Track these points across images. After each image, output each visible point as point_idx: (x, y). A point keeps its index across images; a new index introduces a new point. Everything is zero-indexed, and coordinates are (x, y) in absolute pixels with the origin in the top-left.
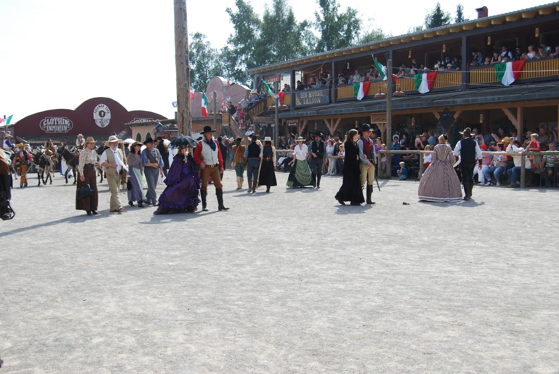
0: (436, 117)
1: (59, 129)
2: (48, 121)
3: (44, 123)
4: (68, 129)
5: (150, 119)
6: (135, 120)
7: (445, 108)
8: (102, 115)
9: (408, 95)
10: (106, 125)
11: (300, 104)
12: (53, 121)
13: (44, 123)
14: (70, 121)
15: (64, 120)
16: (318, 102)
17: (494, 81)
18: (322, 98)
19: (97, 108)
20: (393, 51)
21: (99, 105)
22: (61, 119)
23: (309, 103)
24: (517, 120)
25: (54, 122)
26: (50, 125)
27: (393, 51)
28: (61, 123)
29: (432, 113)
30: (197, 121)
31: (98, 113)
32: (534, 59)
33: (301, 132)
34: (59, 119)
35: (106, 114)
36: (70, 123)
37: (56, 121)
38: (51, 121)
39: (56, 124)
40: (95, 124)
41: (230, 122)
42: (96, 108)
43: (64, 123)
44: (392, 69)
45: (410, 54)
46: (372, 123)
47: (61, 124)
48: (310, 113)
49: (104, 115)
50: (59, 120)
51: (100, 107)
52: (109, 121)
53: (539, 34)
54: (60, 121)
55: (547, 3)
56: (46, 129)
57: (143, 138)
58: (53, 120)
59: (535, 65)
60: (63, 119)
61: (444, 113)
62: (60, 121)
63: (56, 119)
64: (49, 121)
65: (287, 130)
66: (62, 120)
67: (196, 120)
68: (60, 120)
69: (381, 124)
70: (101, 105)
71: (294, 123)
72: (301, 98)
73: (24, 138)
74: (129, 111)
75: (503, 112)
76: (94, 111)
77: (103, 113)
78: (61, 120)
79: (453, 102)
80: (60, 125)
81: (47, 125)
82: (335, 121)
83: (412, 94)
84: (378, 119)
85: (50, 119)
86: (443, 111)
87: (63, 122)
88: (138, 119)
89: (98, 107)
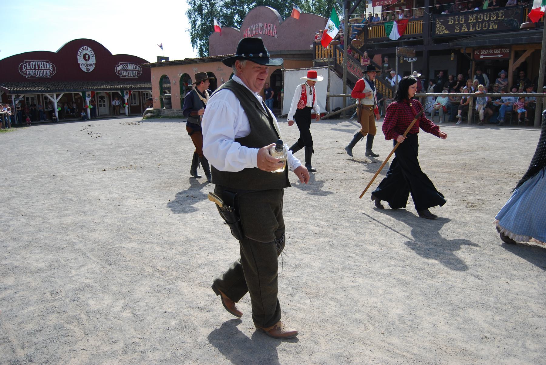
1: (41, 74)
2: (28, 65)
3: (23, 66)
4: (51, 74)
5: (134, 64)
6: (120, 65)
8: (87, 59)
10: (92, 69)
11: (466, 30)
12: (33, 65)
13: (23, 66)
14: (52, 65)
15: (46, 64)
16: (491, 28)
18: (500, 23)
19: (81, 51)
21: (83, 47)
22: (42, 62)
23: (468, 28)
25: (35, 65)
26: (31, 69)
28: (43, 67)
30: (281, 55)
31: (82, 56)
33: (515, 67)
34: (40, 62)
35: (91, 57)
36: (53, 67)
37: (37, 65)
38: (31, 65)
39: (37, 68)
40: (80, 68)
41: (335, 55)
42: (80, 50)
43: (47, 67)
47: (43, 68)
49: (89, 58)
50: (40, 64)
51: (83, 49)
52: (94, 65)
54: (41, 64)
56: (26, 74)
57: (174, 81)
58: (33, 64)
60: (45, 63)
62: (41, 64)
63: (36, 62)
64: (29, 65)
65: (473, 65)
66: (44, 63)
67: (279, 54)
68: (41, 63)
70: (84, 47)
71: (497, 54)
72: (450, 23)
73: (3, 84)
74: (114, 53)
76: (78, 54)
77: (87, 56)
78: (43, 64)
80: (42, 69)
81: (27, 69)
85: (30, 62)
87: (45, 67)
88: (123, 64)
89: (82, 50)
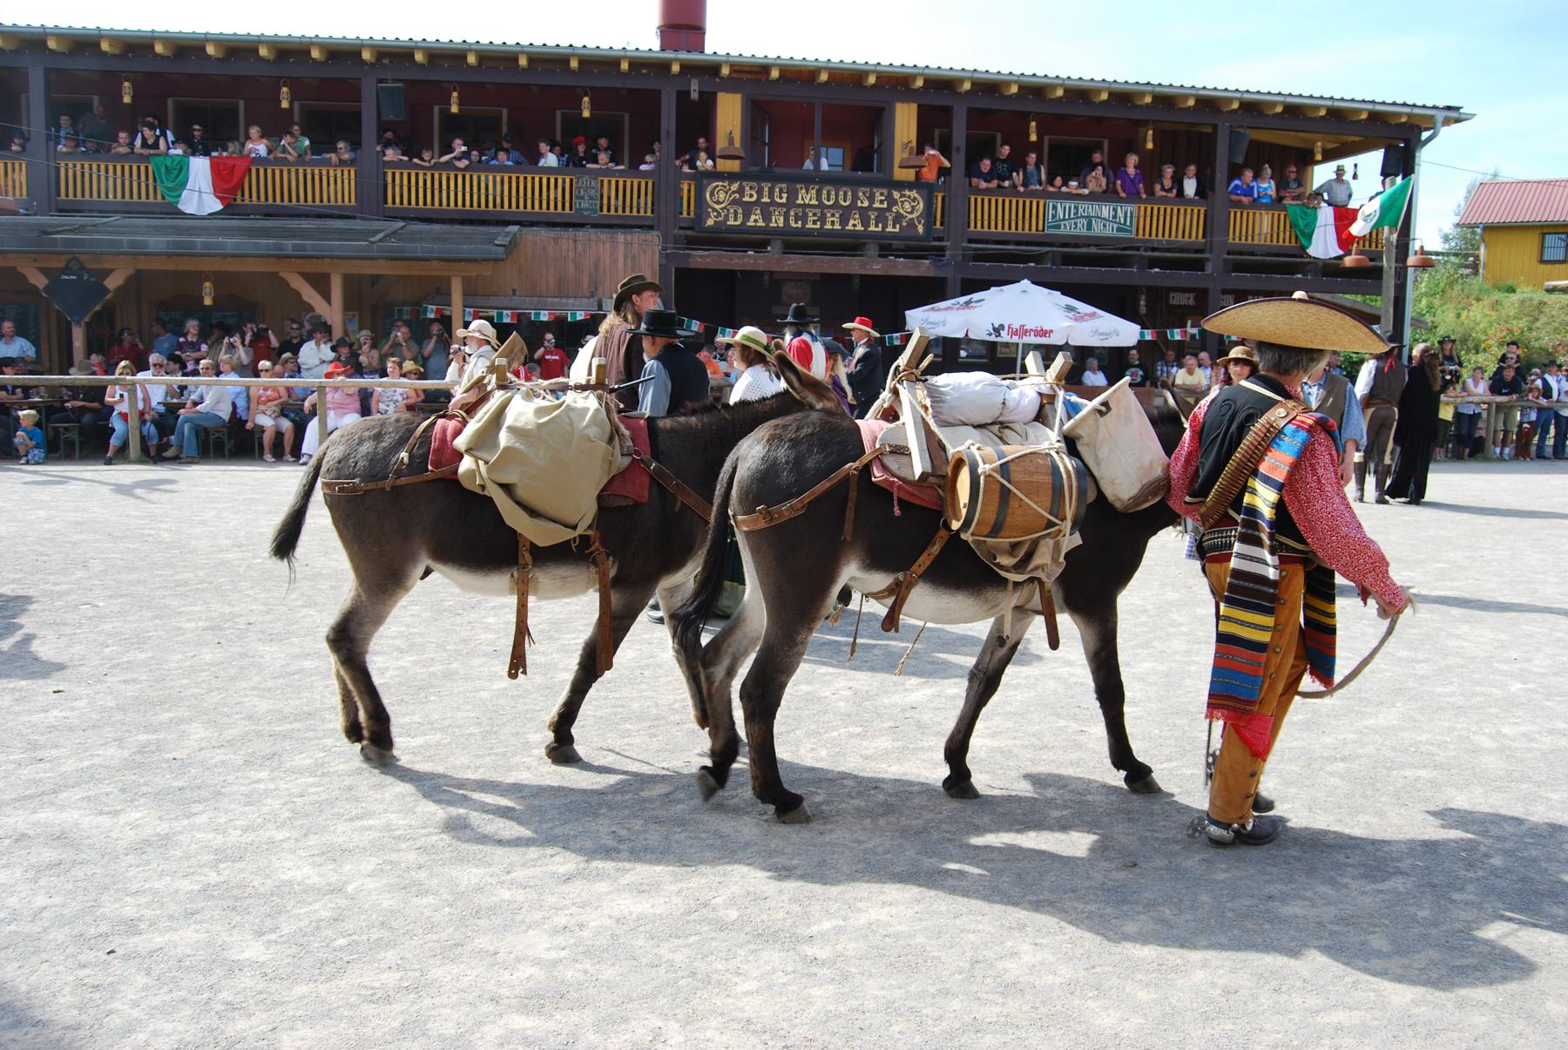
0: (32, 280)
7: (70, 256)
24: (330, 303)
53: (291, 103)
55: (22, 23)
61: (67, 270)
86: (62, 265)
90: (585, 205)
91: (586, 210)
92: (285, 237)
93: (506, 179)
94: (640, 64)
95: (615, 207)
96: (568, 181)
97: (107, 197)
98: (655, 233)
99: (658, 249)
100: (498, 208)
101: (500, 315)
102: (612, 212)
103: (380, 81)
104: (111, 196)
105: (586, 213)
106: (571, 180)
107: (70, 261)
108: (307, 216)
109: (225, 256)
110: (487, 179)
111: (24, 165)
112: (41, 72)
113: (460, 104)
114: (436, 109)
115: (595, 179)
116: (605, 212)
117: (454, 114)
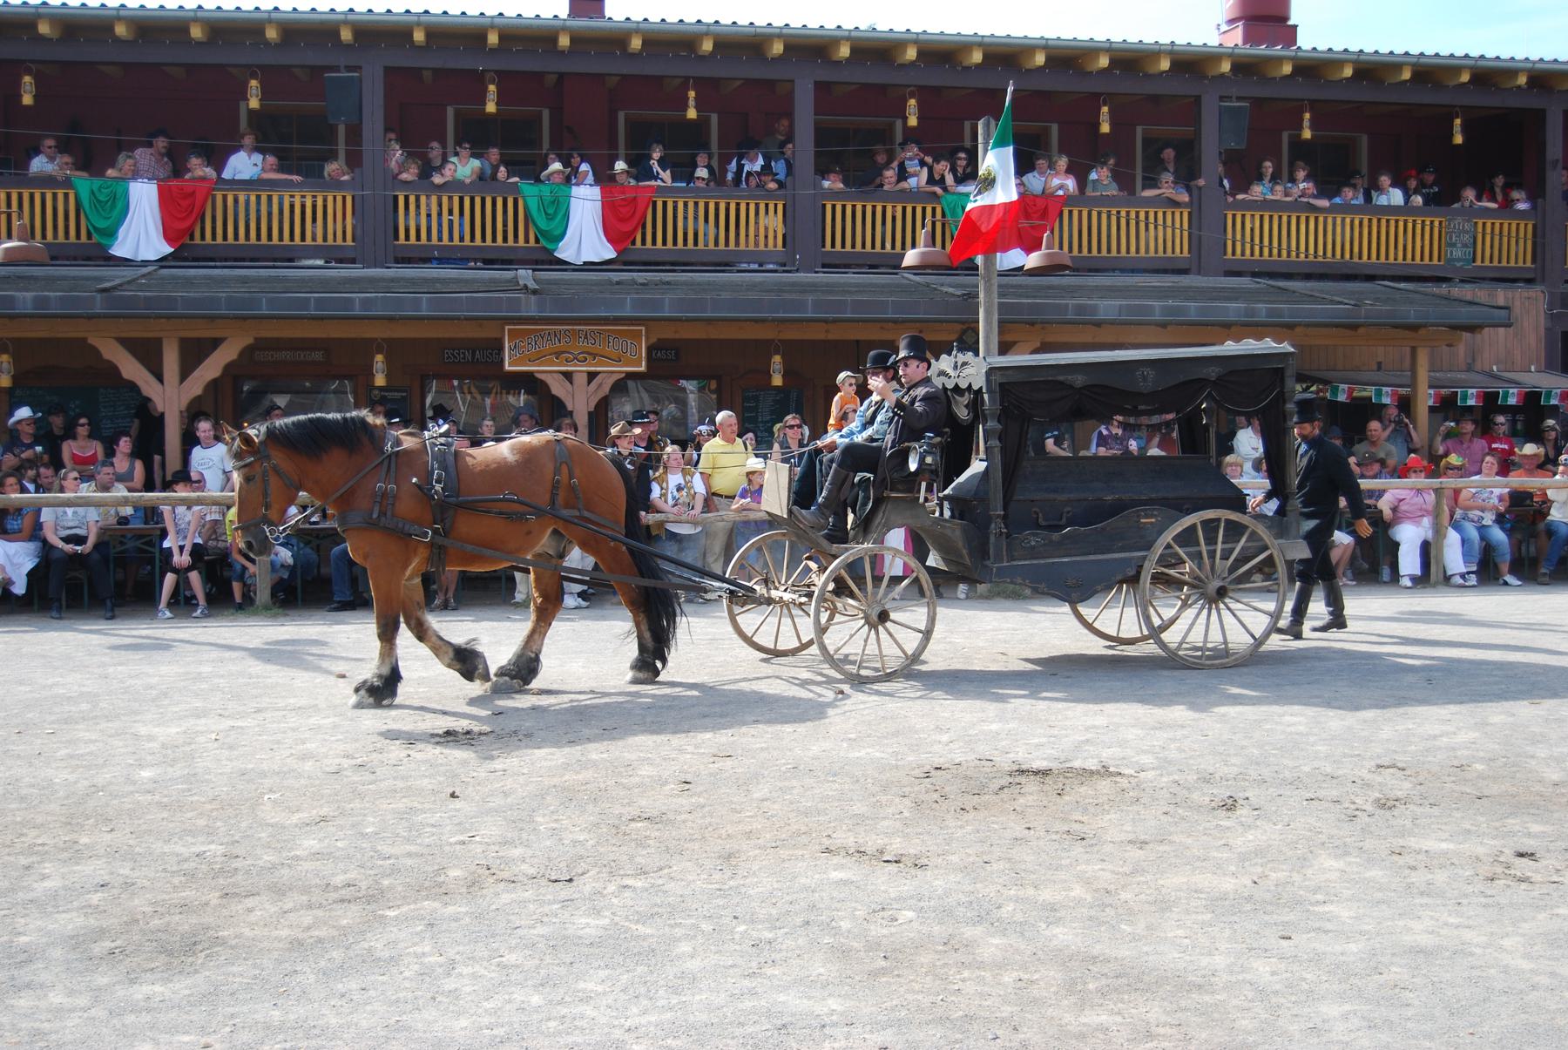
9: (486, 261)
17: (1500, 262)
20: (389, 71)
27: (389, 71)
29: (85, 340)
32: (1391, 210)
44: (364, 144)
45: (692, 102)
46: (507, 368)
48: (41, 302)
59: (325, 207)
69: (568, 376)
75: (95, 351)
79: (1080, 309)
82: (194, 354)
83: (1123, 271)
84: (558, 354)
90: (1457, 253)
91: (1459, 260)
92: (1188, 299)
93: (1366, 222)
94: (1190, 64)
95: (1486, 258)
96: (1436, 224)
97: (883, 247)
98: (1539, 288)
99: (1542, 305)
100: (1356, 260)
101: (1379, 394)
102: (1487, 263)
103: (1222, 98)
104: (888, 246)
105: (1458, 265)
106: (1440, 222)
107: (964, 332)
108: (1165, 271)
109: (1098, 324)
110: (894, 211)
111: (780, 208)
112: (811, 86)
113: (1312, 128)
114: (1285, 136)
115: (1468, 221)
116: (1479, 263)
117: (1307, 141)
